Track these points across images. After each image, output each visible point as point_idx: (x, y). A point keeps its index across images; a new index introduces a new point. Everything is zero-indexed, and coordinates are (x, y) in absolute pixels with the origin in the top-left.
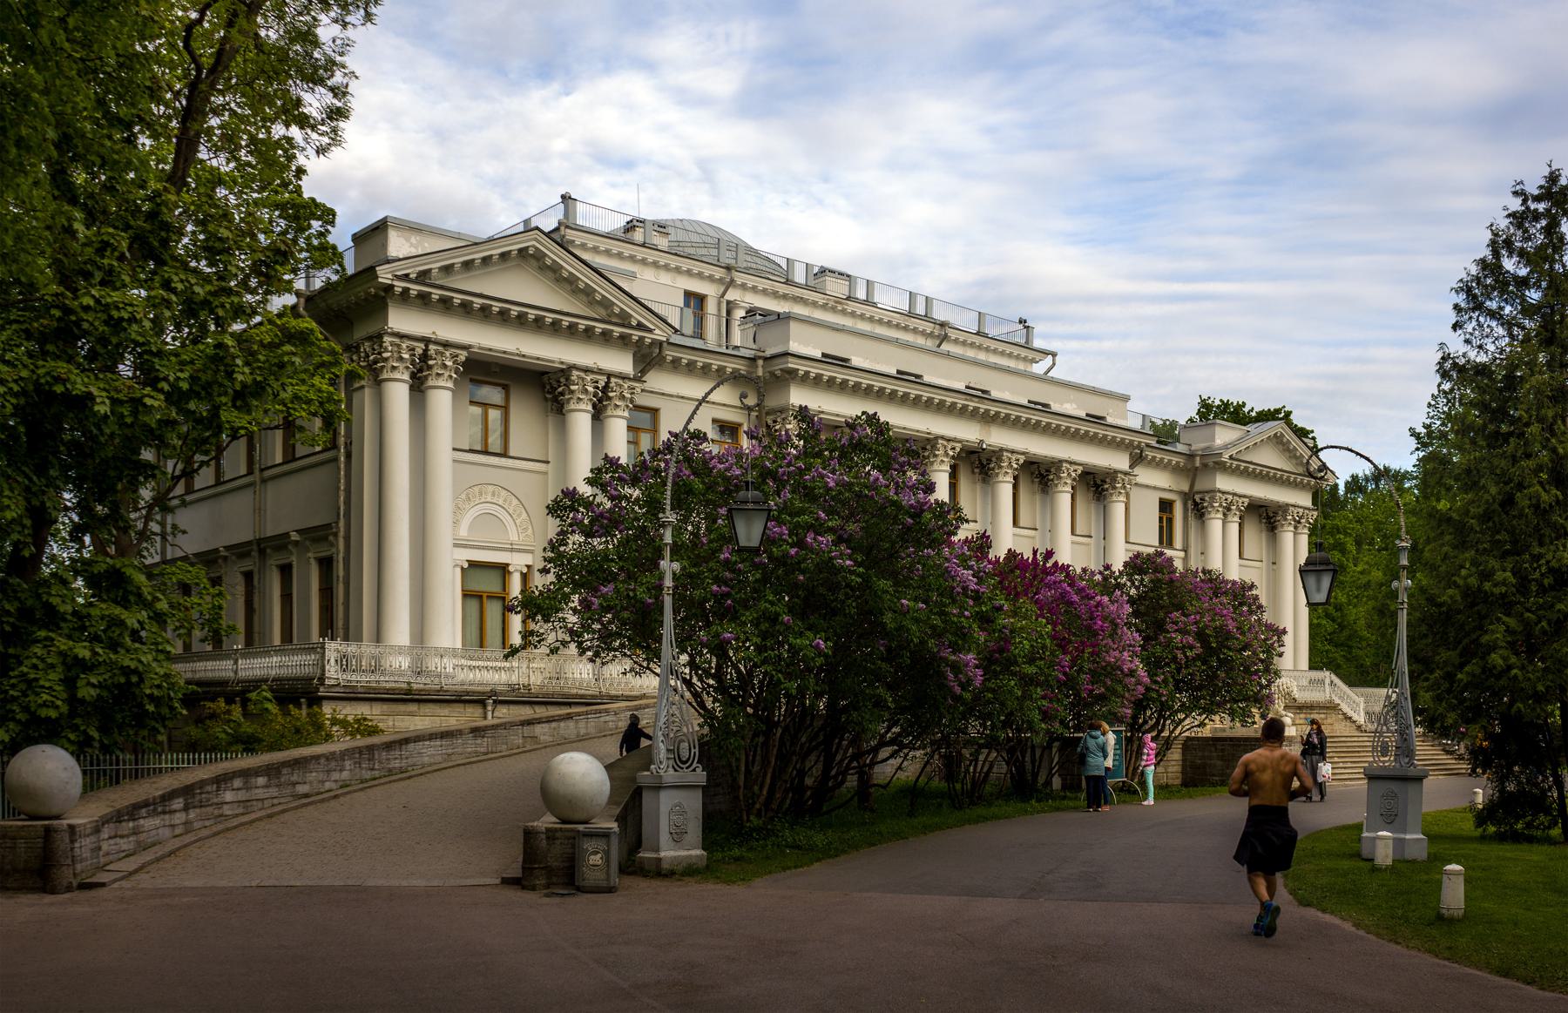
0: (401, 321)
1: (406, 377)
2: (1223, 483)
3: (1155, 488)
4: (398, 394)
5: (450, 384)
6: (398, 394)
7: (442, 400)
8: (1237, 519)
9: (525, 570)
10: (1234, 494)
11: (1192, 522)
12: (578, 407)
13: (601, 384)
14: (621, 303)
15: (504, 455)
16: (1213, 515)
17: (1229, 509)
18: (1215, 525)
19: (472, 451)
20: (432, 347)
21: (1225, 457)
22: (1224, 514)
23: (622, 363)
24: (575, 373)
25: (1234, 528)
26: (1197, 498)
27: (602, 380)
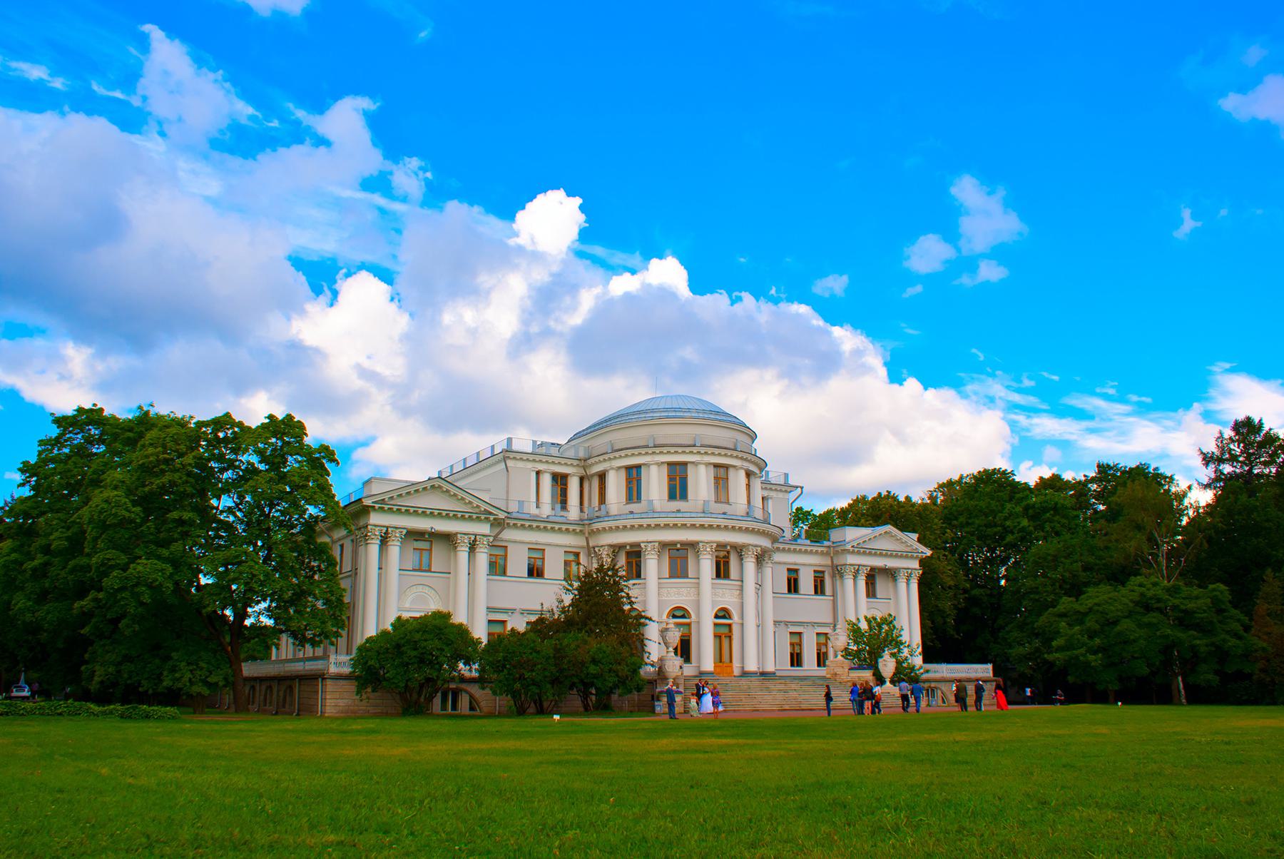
0: (375, 519)
1: (378, 542)
2: (851, 559)
3: (785, 563)
4: (374, 548)
5: (399, 544)
6: (374, 548)
7: (394, 550)
10: (859, 565)
13: (473, 539)
14: (476, 502)
15: (430, 571)
19: (414, 570)
20: (390, 529)
21: (849, 547)
23: (484, 529)
24: (459, 536)
26: (839, 568)
27: (473, 538)
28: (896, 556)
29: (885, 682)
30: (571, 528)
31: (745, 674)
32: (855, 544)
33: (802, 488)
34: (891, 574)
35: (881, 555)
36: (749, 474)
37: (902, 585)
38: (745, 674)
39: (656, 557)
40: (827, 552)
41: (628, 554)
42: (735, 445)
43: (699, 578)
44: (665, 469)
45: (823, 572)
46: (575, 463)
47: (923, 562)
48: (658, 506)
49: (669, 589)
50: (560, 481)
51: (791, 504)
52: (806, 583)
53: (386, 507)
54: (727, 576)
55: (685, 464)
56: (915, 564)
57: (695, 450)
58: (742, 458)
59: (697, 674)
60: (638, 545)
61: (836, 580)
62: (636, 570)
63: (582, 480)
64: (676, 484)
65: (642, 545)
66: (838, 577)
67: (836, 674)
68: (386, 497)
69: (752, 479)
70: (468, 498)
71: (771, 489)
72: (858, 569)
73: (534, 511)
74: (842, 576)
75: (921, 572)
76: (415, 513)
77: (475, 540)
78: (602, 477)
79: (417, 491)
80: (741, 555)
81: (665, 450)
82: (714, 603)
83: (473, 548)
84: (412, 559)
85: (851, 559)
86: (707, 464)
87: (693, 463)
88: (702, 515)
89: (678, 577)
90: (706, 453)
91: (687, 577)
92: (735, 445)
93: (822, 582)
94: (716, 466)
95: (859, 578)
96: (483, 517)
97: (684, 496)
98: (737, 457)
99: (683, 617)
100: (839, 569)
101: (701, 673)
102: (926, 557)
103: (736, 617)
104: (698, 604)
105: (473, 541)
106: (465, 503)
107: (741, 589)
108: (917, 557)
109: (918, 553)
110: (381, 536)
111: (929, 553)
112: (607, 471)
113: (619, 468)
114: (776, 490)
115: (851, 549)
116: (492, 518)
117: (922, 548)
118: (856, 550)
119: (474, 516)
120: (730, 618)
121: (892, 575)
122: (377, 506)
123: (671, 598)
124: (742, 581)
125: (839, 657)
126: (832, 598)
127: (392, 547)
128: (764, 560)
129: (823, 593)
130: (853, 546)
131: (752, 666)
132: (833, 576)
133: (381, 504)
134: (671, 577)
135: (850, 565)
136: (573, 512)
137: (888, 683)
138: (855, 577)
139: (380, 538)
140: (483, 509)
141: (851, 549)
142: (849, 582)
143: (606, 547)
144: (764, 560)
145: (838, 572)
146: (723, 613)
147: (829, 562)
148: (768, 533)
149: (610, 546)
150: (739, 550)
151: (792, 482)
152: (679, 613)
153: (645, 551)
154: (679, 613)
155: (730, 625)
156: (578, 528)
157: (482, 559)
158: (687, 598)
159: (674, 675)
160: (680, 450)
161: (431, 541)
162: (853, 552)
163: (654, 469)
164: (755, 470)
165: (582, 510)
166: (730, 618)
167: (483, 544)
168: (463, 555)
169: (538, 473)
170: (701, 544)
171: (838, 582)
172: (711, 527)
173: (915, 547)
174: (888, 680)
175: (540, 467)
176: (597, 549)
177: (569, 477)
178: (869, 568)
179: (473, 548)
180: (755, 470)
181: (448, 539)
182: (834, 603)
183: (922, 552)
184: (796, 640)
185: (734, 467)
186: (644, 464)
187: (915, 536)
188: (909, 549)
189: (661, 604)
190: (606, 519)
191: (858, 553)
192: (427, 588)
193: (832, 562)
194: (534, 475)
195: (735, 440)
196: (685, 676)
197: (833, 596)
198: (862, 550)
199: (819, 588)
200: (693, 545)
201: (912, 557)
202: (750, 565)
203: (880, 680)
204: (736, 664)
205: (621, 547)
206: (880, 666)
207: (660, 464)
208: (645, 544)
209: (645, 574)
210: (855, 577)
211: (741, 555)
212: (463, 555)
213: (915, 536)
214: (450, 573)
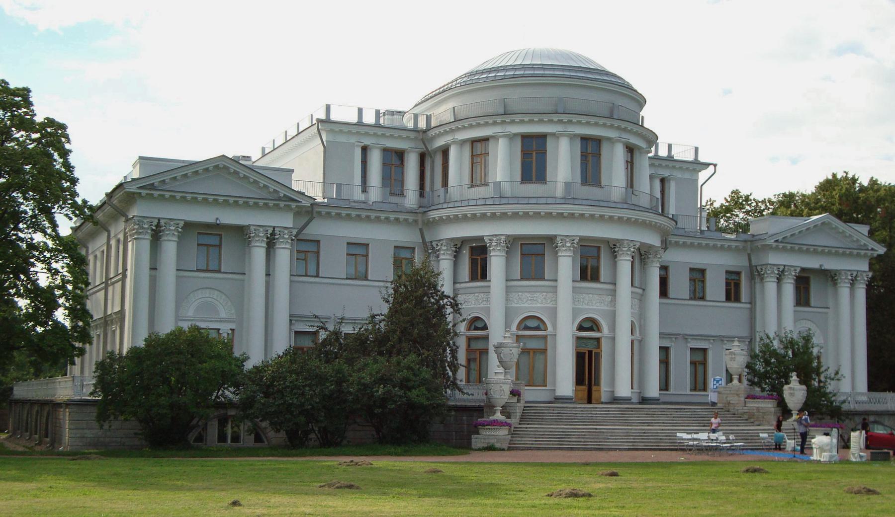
2: (775, 259)
7: (170, 247)
9: (230, 332)
10: (784, 266)
12: (256, 245)
14: (272, 187)
15: (219, 271)
16: (842, 285)
19: (198, 270)
20: (162, 222)
21: (771, 242)
23: (285, 221)
25: (789, 289)
28: (837, 254)
29: (791, 415)
30: (402, 217)
31: (615, 400)
32: (780, 238)
33: (715, 165)
34: (830, 277)
35: (815, 252)
36: (631, 150)
37: (844, 291)
38: (615, 400)
39: (504, 254)
40: (744, 247)
41: (473, 250)
42: (612, 112)
43: (556, 280)
44: (578, 144)
45: (738, 274)
46: (412, 135)
47: (876, 262)
48: (506, 189)
49: (520, 293)
51: (702, 186)
52: (715, 287)
53: (156, 193)
54: (595, 278)
56: (864, 266)
57: (555, 118)
58: (619, 128)
59: (553, 400)
60: (481, 238)
61: (755, 283)
62: (480, 272)
63: (422, 157)
64: (531, 162)
65: (486, 239)
67: (729, 403)
68: (156, 181)
69: (637, 155)
70: (263, 182)
71: (674, 167)
72: (783, 270)
73: (358, 195)
74: (762, 279)
75: (870, 274)
76: (193, 201)
77: (273, 234)
78: (445, 152)
79: (196, 173)
80: (615, 252)
82: (575, 312)
83: (271, 244)
84: (194, 258)
85: (775, 259)
86: (572, 137)
87: (553, 134)
88: (562, 201)
89: (533, 279)
90: (570, 122)
91: (543, 279)
92: (612, 112)
93: (737, 285)
94: (585, 139)
95: (785, 281)
96: (282, 204)
97: (541, 178)
98: (612, 126)
99: (537, 328)
100: (759, 270)
101: (558, 399)
103: (605, 330)
104: (554, 312)
105: (271, 234)
106: (260, 188)
107: (613, 293)
108: (865, 255)
109: (868, 250)
110: (153, 230)
111: (881, 250)
113: (464, 142)
114: (681, 168)
115: (774, 245)
116: (294, 205)
117: (872, 244)
118: (781, 245)
119: (271, 203)
120: (599, 330)
121: (833, 278)
122: (144, 192)
123: (522, 305)
126: (748, 306)
127: (166, 242)
128: (649, 258)
129: (737, 299)
130: (777, 241)
131: (624, 389)
132: (752, 278)
133: (150, 189)
134: (522, 279)
136: (411, 198)
138: (779, 280)
139: (176, 234)
140: (282, 195)
141: (774, 245)
142: (771, 286)
144: (649, 258)
145: (756, 274)
146: (589, 325)
147: (746, 263)
148: (660, 227)
150: (613, 247)
151: (702, 159)
152: (532, 323)
153: (490, 247)
154: (532, 323)
155: (598, 340)
156: (411, 218)
157: (283, 255)
158: (542, 305)
159: (503, 403)
160: (536, 118)
161: (220, 235)
162: (777, 248)
163: (502, 144)
164: (642, 144)
165: (422, 195)
166: (599, 330)
167: (284, 238)
168: (259, 253)
169: (365, 149)
170: (558, 239)
171: (758, 286)
172: (572, 216)
173: (863, 242)
174: (795, 413)
175: (367, 141)
176: (434, 244)
177: (406, 155)
178: (798, 270)
179: (271, 244)
180: (642, 144)
181: (241, 233)
183: (872, 249)
184: (699, 357)
185: (609, 139)
186: (492, 137)
187: (864, 229)
188: (854, 245)
189: (509, 313)
190: (445, 206)
191: (784, 249)
192: (208, 291)
194: (358, 153)
195: (611, 105)
196: (526, 402)
197: (750, 303)
198: (789, 246)
199: (732, 293)
201: (858, 255)
202: (624, 266)
204: (604, 387)
205: (464, 241)
206: (786, 395)
207: (512, 137)
208: (489, 237)
209: (490, 276)
210: (779, 280)
211: (615, 252)
212: (259, 253)
213: (864, 229)
214: (245, 274)
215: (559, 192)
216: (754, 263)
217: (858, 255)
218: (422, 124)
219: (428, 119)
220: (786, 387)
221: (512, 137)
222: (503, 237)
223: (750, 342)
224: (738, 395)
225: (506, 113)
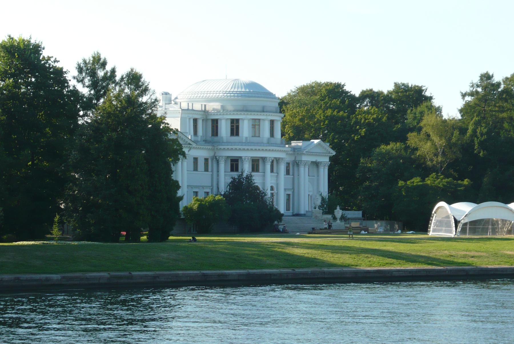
8: (308, 167)
11: (296, 168)
17: (306, 164)
18: (302, 169)
21: (304, 152)
22: (304, 166)
25: (307, 169)
26: (297, 162)
32: (307, 150)
43: (264, 173)
46: (202, 113)
47: (331, 159)
50: (195, 121)
55: (259, 120)
56: (327, 160)
60: (241, 157)
63: (203, 120)
66: (296, 166)
67: (317, 216)
74: (298, 165)
81: (253, 113)
85: (305, 158)
100: (297, 162)
102: (333, 155)
104: (264, 184)
109: (330, 153)
112: (221, 120)
113: (227, 119)
124: (278, 173)
125: (317, 208)
130: (306, 152)
132: (293, 166)
135: (304, 161)
137: (338, 221)
143: (224, 157)
145: (297, 164)
149: (225, 156)
150: (278, 160)
171: (296, 168)
173: (329, 150)
174: (338, 219)
182: (293, 179)
183: (332, 153)
188: (325, 152)
193: (295, 159)
194: (188, 120)
200: (264, 159)
203: (335, 218)
205: (228, 157)
207: (249, 120)
215: (265, 141)
216: (296, 159)
217: (326, 155)
218: (203, 109)
219: (205, 106)
220: (335, 210)
221: (249, 120)
222: (250, 157)
223: (293, 191)
224: (320, 213)
225: (245, 110)
